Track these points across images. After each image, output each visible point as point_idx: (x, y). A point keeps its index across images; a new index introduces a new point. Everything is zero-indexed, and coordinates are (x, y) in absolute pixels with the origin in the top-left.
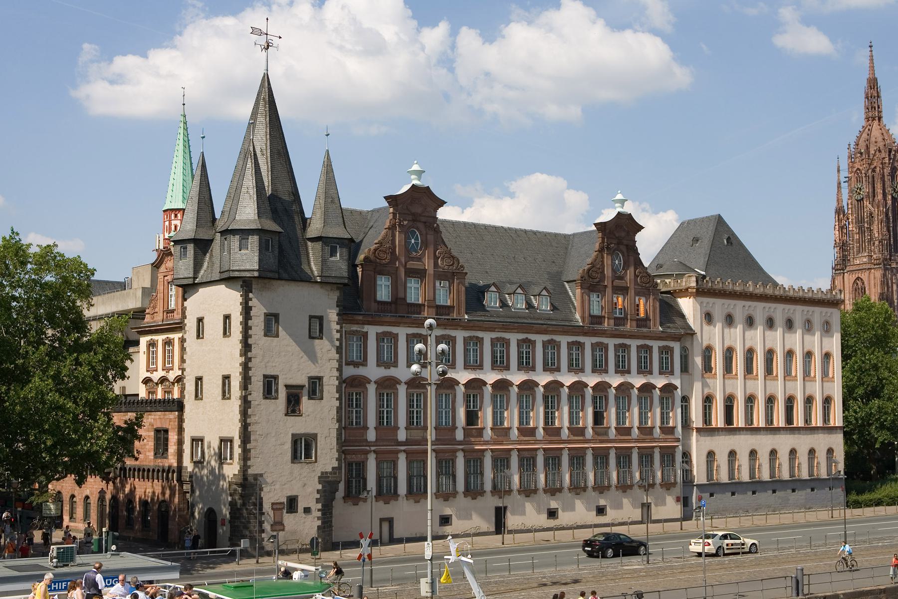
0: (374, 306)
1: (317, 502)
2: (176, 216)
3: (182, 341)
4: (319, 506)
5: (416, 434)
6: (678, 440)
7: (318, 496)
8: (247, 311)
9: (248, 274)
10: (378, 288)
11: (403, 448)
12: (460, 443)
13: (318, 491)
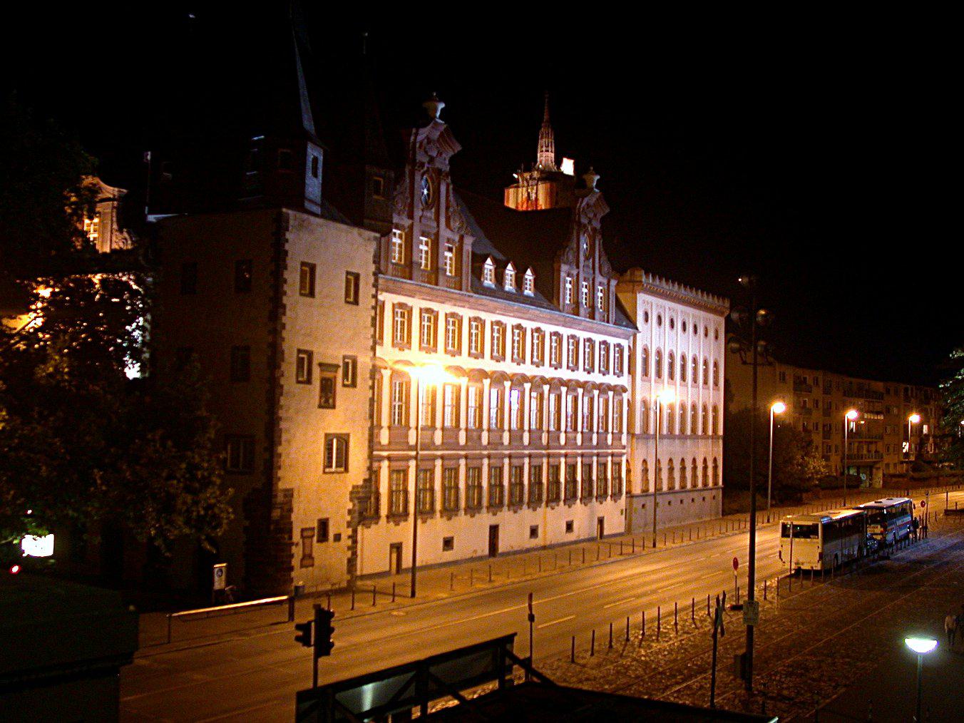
1: (348, 527)
4: (350, 532)
6: (624, 447)
7: (349, 518)
13: (350, 512)
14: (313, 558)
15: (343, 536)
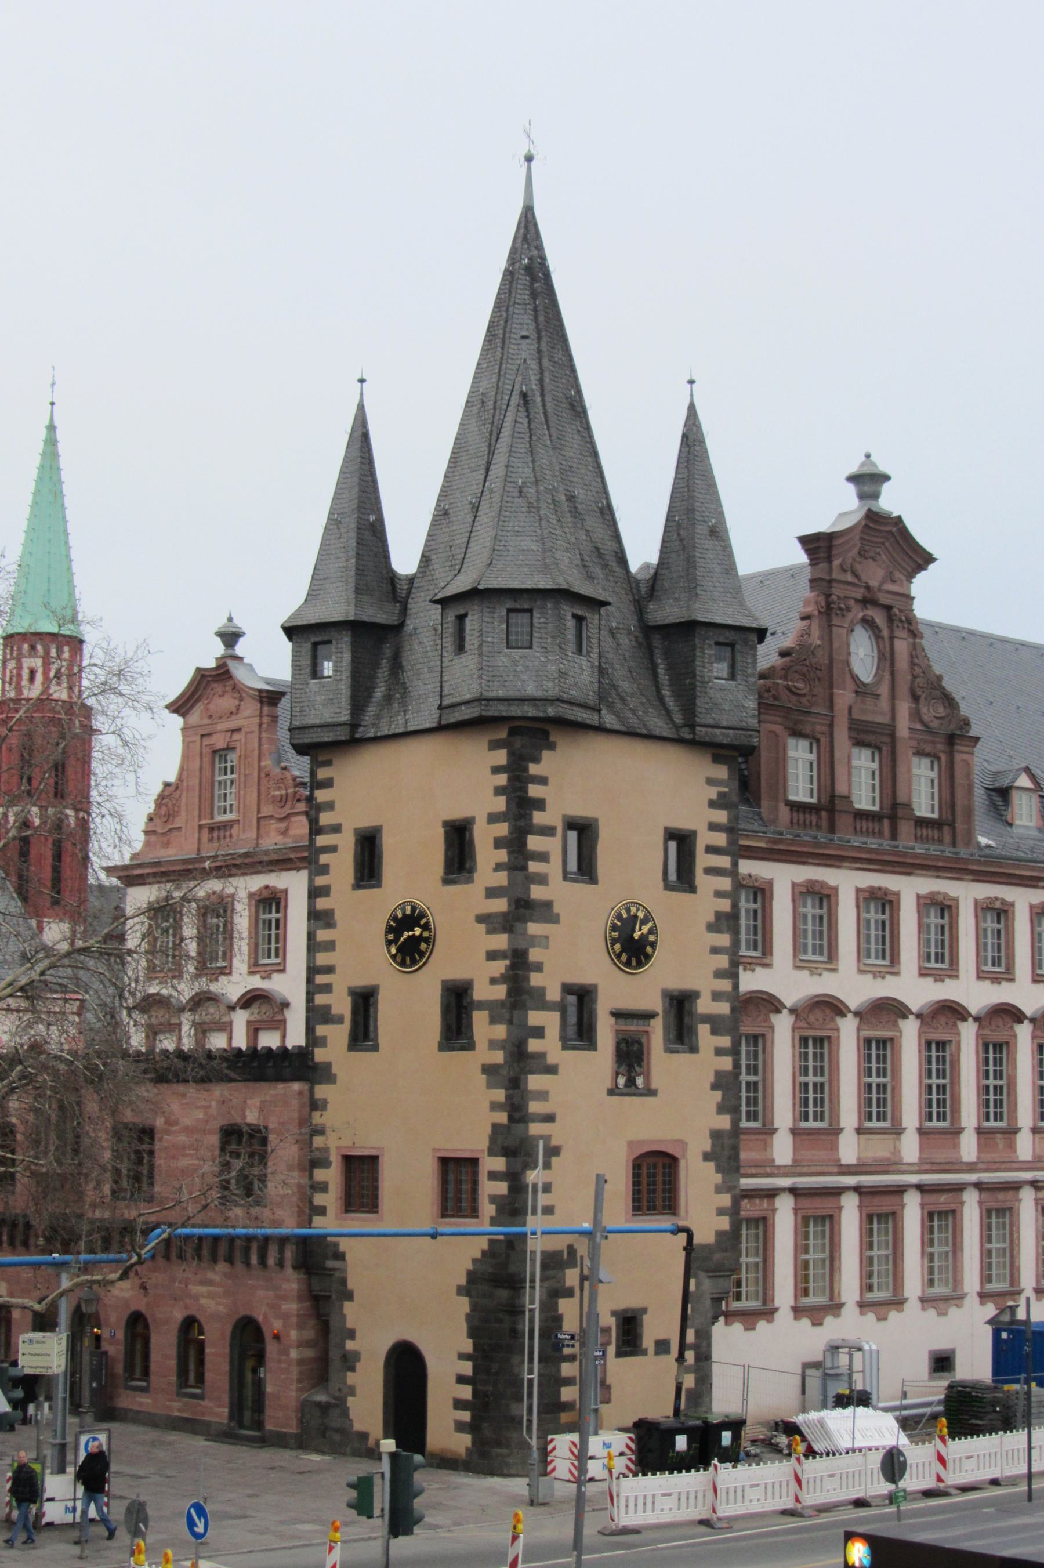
0: (784, 812)
2: (33, 648)
3: (315, 892)
5: (879, 1149)
8: (520, 806)
9: (531, 711)
10: (791, 764)
11: (851, 1181)
12: (971, 1168)
14: (609, 1387)
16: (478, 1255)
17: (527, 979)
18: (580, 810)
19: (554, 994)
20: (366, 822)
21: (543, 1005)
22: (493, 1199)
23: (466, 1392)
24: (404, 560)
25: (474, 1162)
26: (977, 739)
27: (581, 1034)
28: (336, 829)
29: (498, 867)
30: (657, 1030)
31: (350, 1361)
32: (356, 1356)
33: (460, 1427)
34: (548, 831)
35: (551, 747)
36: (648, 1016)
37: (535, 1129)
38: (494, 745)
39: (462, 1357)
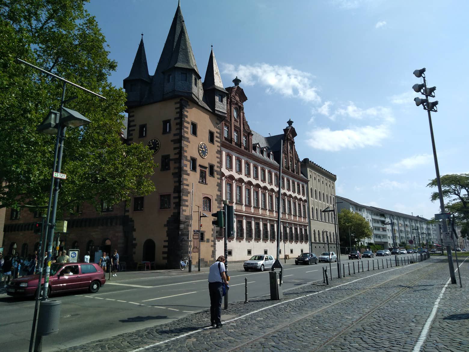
7: (212, 233)
15: (210, 241)
16: (170, 216)
17: (184, 153)
18: (195, 121)
19: (189, 158)
20: (143, 123)
21: (187, 160)
22: (174, 203)
23: (166, 250)
24: (152, 72)
25: (170, 195)
26: (253, 135)
27: (194, 169)
28: (135, 126)
29: (177, 129)
30: (207, 171)
31: (134, 246)
32: (136, 244)
33: (164, 258)
34: (188, 123)
35: (189, 105)
36: (206, 168)
37: (185, 187)
38: (176, 103)
39: (165, 241)
